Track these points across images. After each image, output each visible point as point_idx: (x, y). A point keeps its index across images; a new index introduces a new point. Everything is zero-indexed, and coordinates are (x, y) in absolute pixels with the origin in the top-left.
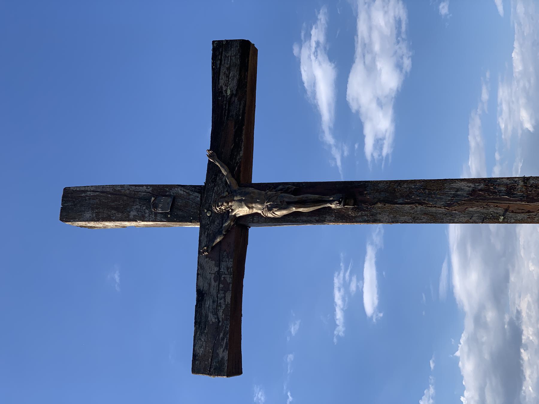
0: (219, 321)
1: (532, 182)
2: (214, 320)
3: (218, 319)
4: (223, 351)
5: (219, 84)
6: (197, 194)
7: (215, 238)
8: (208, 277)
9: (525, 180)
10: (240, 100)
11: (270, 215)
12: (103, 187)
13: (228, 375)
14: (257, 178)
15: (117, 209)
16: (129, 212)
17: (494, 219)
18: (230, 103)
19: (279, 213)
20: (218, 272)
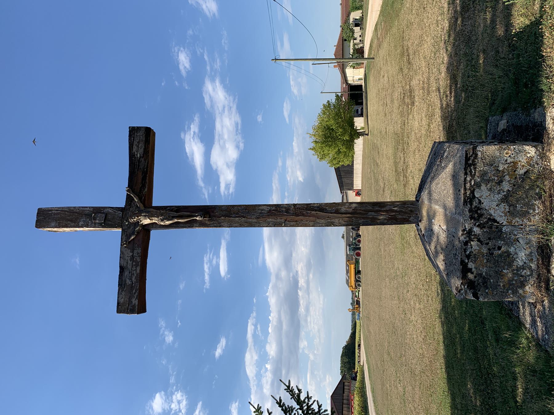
0: (133, 283)
1: (298, 206)
2: (129, 283)
3: (132, 282)
4: (135, 300)
5: (133, 150)
6: (120, 212)
7: (130, 237)
8: (127, 258)
10: (145, 160)
11: (162, 224)
12: (63, 208)
14: (156, 203)
15: (71, 221)
16: (79, 222)
18: (139, 161)
19: (168, 223)
20: (133, 255)
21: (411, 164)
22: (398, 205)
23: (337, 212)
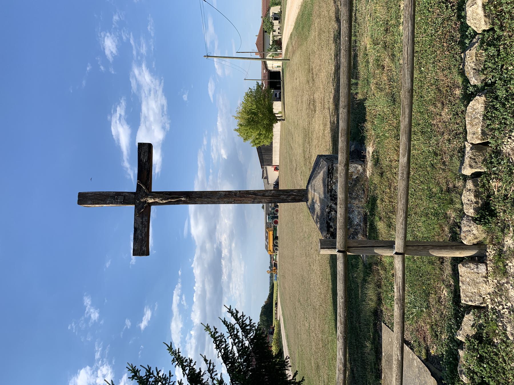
6: (133, 195)
7: (141, 210)
8: (138, 223)
9: (240, 191)
10: (148, 163)
11: (161, 202)
12: (95, 192)
13: (146, 256)
14: (154, 189)
15: (102, 200)
17: (231, 203)
18: (145, 164)
19: (164, 202)
20: (142, 221)
21: (313, 154)
22: (296, 192)
23: (264, 195)
